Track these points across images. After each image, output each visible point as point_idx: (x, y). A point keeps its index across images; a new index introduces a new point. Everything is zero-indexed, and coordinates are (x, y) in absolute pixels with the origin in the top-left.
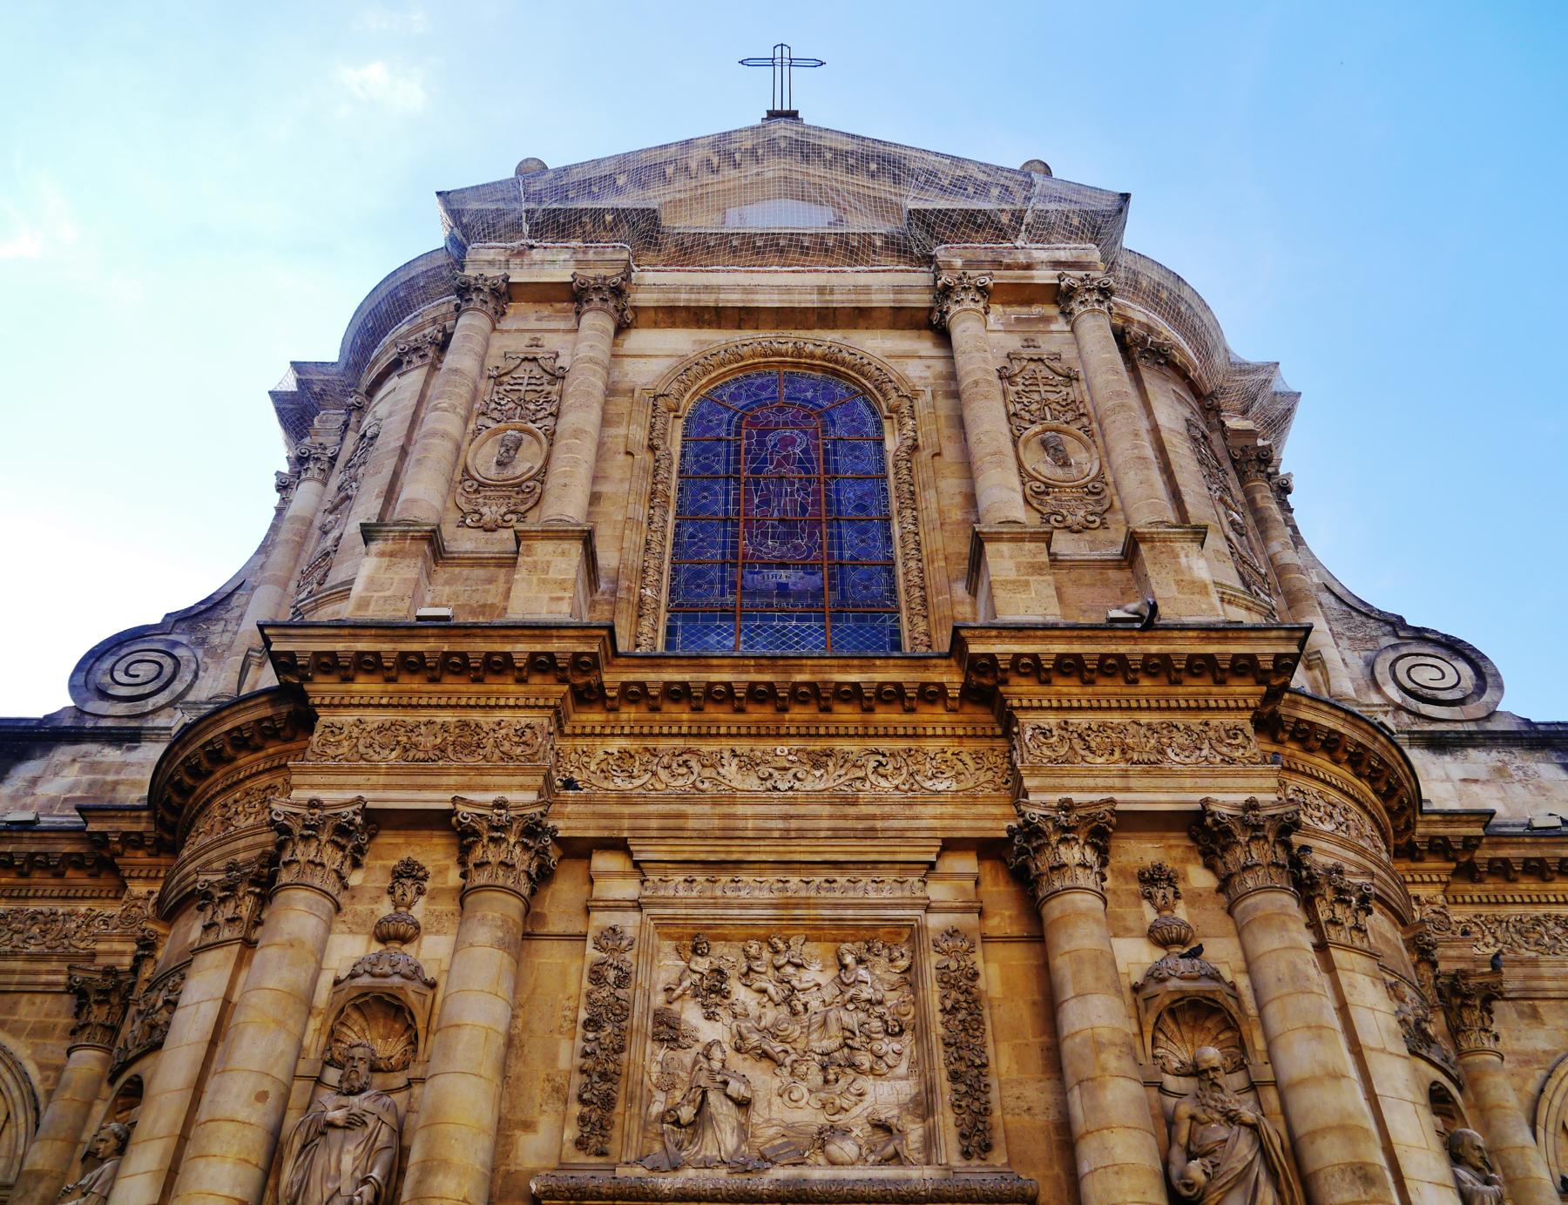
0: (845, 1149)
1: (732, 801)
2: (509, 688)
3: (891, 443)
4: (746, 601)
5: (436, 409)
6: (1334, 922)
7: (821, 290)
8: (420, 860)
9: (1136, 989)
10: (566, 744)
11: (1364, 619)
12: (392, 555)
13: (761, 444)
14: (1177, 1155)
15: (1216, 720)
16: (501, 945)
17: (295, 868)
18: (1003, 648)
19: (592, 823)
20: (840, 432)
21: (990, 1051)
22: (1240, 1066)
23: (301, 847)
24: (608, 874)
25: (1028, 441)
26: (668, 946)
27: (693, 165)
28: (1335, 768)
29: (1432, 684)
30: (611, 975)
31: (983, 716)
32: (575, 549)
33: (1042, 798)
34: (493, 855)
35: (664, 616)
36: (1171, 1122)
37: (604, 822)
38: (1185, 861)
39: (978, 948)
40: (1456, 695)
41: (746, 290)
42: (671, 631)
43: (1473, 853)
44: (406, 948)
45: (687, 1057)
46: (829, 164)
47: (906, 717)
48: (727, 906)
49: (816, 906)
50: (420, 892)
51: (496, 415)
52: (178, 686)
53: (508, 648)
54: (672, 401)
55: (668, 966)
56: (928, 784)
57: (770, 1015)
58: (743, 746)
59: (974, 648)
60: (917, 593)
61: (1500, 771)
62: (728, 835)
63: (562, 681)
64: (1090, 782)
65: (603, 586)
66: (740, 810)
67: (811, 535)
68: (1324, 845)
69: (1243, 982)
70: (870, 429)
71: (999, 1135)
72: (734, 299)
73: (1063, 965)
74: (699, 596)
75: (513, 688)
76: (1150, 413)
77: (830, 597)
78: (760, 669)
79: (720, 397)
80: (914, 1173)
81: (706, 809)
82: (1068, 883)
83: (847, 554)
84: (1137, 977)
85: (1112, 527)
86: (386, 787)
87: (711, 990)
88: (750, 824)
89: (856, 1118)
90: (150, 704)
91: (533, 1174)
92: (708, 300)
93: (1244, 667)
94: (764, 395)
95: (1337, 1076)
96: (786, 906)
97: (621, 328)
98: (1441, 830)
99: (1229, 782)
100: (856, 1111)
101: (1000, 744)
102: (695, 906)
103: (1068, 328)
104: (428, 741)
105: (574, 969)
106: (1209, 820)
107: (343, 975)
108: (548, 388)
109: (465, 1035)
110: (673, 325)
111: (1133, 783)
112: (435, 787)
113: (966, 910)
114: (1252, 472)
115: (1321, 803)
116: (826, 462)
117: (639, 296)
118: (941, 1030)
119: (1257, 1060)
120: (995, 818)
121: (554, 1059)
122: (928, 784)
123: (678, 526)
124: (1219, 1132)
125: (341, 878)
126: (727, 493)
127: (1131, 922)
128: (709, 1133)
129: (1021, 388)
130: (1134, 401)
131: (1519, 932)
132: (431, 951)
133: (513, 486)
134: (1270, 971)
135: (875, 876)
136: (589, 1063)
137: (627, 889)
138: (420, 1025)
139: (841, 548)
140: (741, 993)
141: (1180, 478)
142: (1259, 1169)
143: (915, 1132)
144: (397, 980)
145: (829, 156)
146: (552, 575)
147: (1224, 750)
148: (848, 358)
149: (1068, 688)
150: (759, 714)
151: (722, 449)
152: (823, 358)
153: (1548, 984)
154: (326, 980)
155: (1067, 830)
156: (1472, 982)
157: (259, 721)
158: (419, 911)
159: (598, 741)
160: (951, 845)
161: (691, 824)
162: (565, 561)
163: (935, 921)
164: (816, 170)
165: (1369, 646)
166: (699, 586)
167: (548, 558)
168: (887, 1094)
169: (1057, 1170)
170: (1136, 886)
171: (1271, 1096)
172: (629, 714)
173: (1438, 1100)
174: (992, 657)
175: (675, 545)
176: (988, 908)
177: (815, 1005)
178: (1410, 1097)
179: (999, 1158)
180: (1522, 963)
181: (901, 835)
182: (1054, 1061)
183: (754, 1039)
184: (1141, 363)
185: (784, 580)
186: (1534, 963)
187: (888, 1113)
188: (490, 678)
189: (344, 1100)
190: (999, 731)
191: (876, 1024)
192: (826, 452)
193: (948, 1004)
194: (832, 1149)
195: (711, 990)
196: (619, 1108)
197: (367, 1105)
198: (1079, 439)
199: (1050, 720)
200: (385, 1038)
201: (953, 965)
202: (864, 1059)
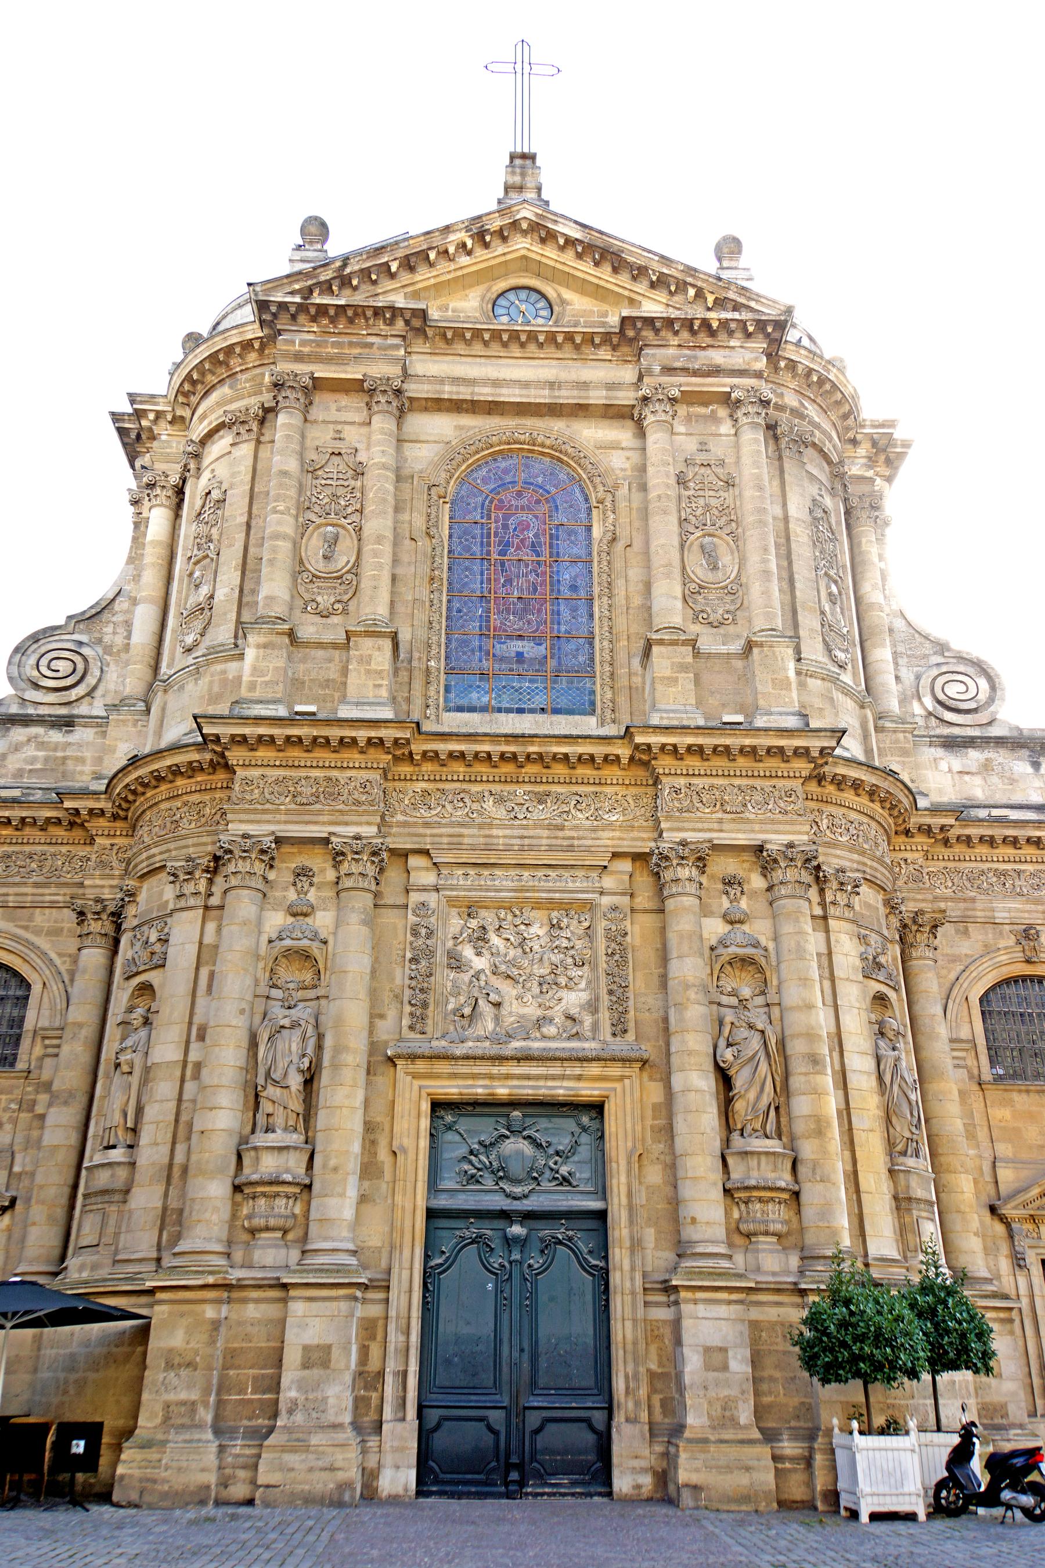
0: (551, 1030)
1: (490, 826)
2: (354, 757)
3: (597, 532)
4: (497, 666)
5: (275, 511)
6: (833, 903)
7: (552, 385)
8: (308, 863)
9: (712, 949)
10: (390, 784)
11: (923, 640)
12: (265, 646)
13: (505, 527)
14: (722, 1043)
15: (780, 783)
16: (364, 923)
17: (239, 876)
18: (656, 740)
19: (408, 839)
20: (561, 518)
21: (631, 978)
22: (763, 993)
23: (240, 862)
24: (418, 869)
25: (692, 544)
26: (454, 911)
27: (451, 250)
28: (857, 799)
29: (957, 696)
30: (423, 931)
31: (641, 773)
32: (387, 644)
33: (672, 837)
34: (355, 869)
35: (443, 677)
36: (721, 1023)
37: (415, 839)
38: (750, 870)
39: (629, 918)
40: (972, 705)
41: (496, 383)
42: (447, 689)
43: (952, 831)
44: (309, 920)
45: (466, 977)
46: (562, 248)
47: (595, 772)
48: (487, 890)
49: (538, 891)
50: (311, 885)
51: (317, 509)
52: (91, 680)
53: (353, 733)
54: (442, 492)
55: (456, 923)
56: (606, 817)
57: (512, 953)
58: (496, 788)
59: (639, 739)
60: (607, 668)
61: (987, 767)
62: (488, 848)
63: (389, 753)
64: (700, 825)
65: (402, 656)
66: (495, 832)
67: (539, 611)
68: (838, 852)
69: (771, 946)
70: (583, 516)
71: (631, 1025)
72: (485, 393)
73: (672, 937)
74: (465, 662)
75: (357, 756)
76: (784, 505)
77: (551, 664)
78: (507, 743)
79: (475, 480)
80: (586, 1045)
81: (475, 831)
82: (680, 890)
83: (563, 628)
84: (714, 942)
85: (740, 622)
86: (286, 822)
87: (478, 939)
88: (501, 841)
89: (557, 1013)
90: (74, 694)
91: (386, 1042)
92: (464, 393)
93: (802, 753)
94: (508, 479)
95: (810, 1007)
96: (521, 891)
97: (401, 414)
98: (928, 820)
99: (781, 827)
100: (557, 1008)
101: (650, 790)
102: (470, 890)
103: (733, 431)
104: (308, 791)
105: (400, 924)
106: (765, 854)
107: (274, 936)
108: (352, 483)
109: (350, 976)
110: (439, 410)
111: (725, 826)
112: (316, 823)
113: (623, 894)
114: (864, 515)
115: (844, 821)
116: (551, 546)
117: (413, 386)
118: (605, 966)
119: (772, 990)
120: (643, 840)
121: (393, 979)
122: (606, 817)
123: (449, 601)
124: (743, 1033)
125: (265, 878)
126: (482, 574)
127: (714, 908)
128: (479, 1024)
129: (691, 492)
130: (772, 487)
131: (969, 880)
132: (323, 920)
133: (338, 578)
134: (788, 943)
135: (572, 872)
136: (414, 983)
137: (429, 878)
138: (321, 966)
139: (559, 624)
140: (495, 940)
141: (796, 568)
142: (762, 1055)
143: (588, 1020)
144: (305, 942)
145: (561, 241)
146: (373, 666)
147: (782, 805)
148: (570, 450)
149: (693, 763)
150: (508, 768)
151: (478, 532)
152: (551, 447)
153: (979, 914)
154: (264, 939)
155: (683, 858)
156: (927, 916)
157: (191, 763)
158: (312, 895)
159: (408, 784)
160: (615, 855)
161: (466, 840)
162: (381, 655)
163: (606, 901)
164: (550, 254)
165: (922, 662)
166: (464, 653)
167: (369, 652)
168: (574, 999)
169: (661, 1043)
170: (720, 886)
171: (776, 1011)
172: (428, 767)
173: (880, 999)
174: (649, 746)
175: (447, 618)
176: (637, 892)
177: (536, 948)
178: (857, 1005)
179: (631, 1036)
180: (965, 900)
181: (588, 850)
182: (664, 981)
183: (503, 968)
184: (786, 453)
185: (520, 650)
186: (973, 900)
187: (574, 1011)
188: (343, 750)
189: (287, 1012)
190: (650, 782)
191: (570, 960)
192: (551, 535)
193: (610, 951)
194: (544, 1030)
195: (478, 939)
196: (431, 1008)
197: (299, 1014)
198: (728, 544)
199: (682, 781)
200: (300, 970)
201: (614, 928)
202: (563, 980)
